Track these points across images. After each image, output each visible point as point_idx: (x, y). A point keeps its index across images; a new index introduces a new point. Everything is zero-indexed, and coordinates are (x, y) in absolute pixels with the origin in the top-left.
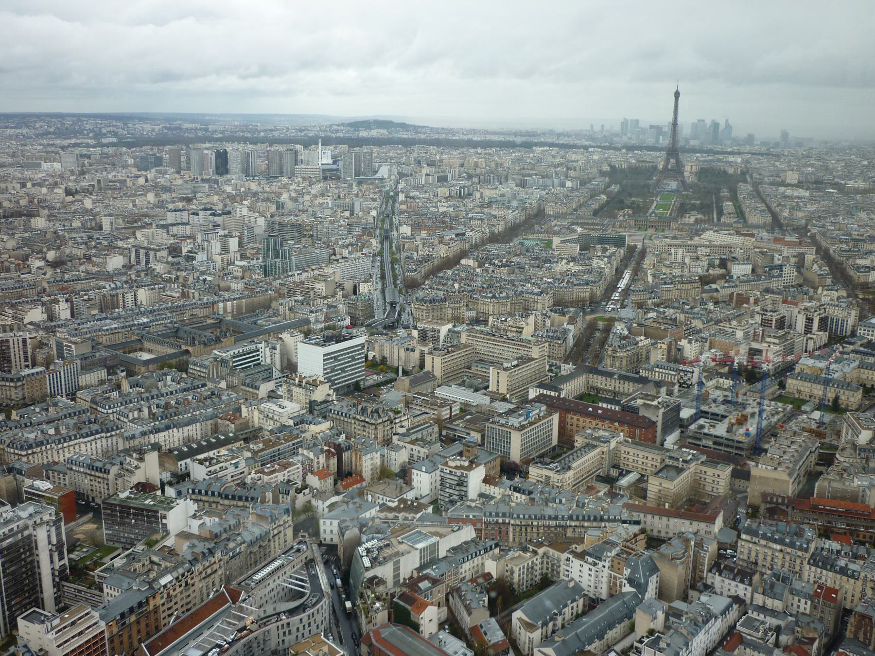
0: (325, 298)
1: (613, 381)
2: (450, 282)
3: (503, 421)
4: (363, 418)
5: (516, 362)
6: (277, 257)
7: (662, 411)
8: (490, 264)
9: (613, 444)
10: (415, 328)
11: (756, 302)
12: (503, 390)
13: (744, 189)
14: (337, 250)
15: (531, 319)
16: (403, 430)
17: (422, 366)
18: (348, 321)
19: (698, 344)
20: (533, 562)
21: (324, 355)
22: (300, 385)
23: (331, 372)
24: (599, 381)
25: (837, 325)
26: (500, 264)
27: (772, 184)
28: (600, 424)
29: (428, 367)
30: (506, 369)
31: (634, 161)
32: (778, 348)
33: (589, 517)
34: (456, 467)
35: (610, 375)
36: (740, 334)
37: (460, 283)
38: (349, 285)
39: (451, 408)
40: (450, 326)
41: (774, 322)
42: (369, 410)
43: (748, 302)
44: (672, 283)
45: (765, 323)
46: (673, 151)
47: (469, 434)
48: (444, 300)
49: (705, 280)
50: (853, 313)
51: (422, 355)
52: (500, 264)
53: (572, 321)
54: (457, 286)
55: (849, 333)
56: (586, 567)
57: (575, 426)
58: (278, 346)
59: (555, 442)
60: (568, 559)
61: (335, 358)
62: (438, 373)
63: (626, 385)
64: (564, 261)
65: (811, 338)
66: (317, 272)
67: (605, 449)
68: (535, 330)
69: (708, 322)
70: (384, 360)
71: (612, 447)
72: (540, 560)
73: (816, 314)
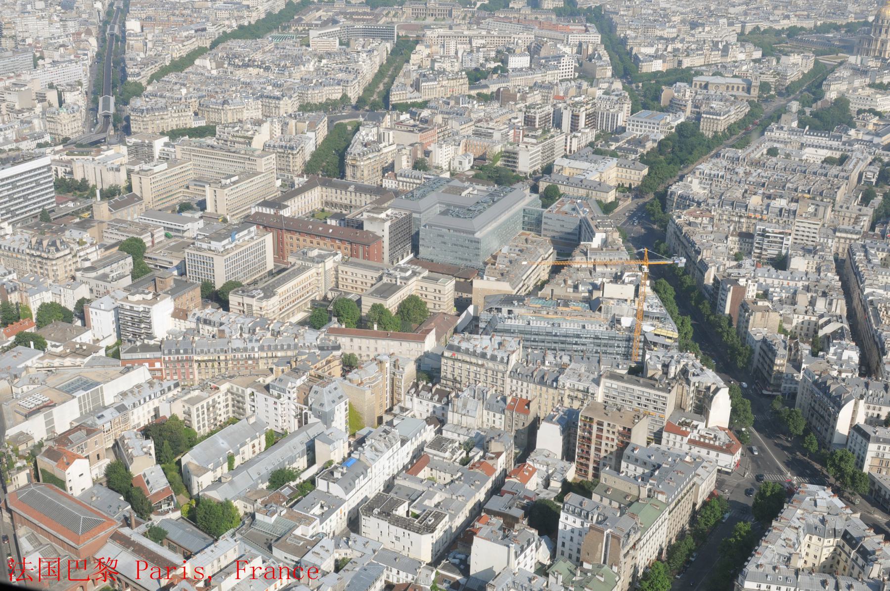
0: (21, 111)
1: (348, 193)
2: (178, 86)
4: (38, 253)
5: (236, 178)
7: (388, 224)
10: (125, 144)
12: (222, 211)
14: (46, 53)
16: (87, 264)
17: (129, 188)
20: (214, 400)
23: (10, 201)
28: (322, 242)
29: (136, 190)
33: (282, 346)
34: (138, 302)
35: (345, 187)
37: (188, 88)
38: (52, 96)
39: (152, 236)
41: (537, 120)
43: (514, 99)
51: (129, 172)
56: (271, 400)
57: (295, 245)
60: (253, 394)
61: (14, 185)
62: (148, 196)
66: (13, 81)
68: (271, 138)
70: (84, 181)
72: (223, 398)
73: (583, 109)
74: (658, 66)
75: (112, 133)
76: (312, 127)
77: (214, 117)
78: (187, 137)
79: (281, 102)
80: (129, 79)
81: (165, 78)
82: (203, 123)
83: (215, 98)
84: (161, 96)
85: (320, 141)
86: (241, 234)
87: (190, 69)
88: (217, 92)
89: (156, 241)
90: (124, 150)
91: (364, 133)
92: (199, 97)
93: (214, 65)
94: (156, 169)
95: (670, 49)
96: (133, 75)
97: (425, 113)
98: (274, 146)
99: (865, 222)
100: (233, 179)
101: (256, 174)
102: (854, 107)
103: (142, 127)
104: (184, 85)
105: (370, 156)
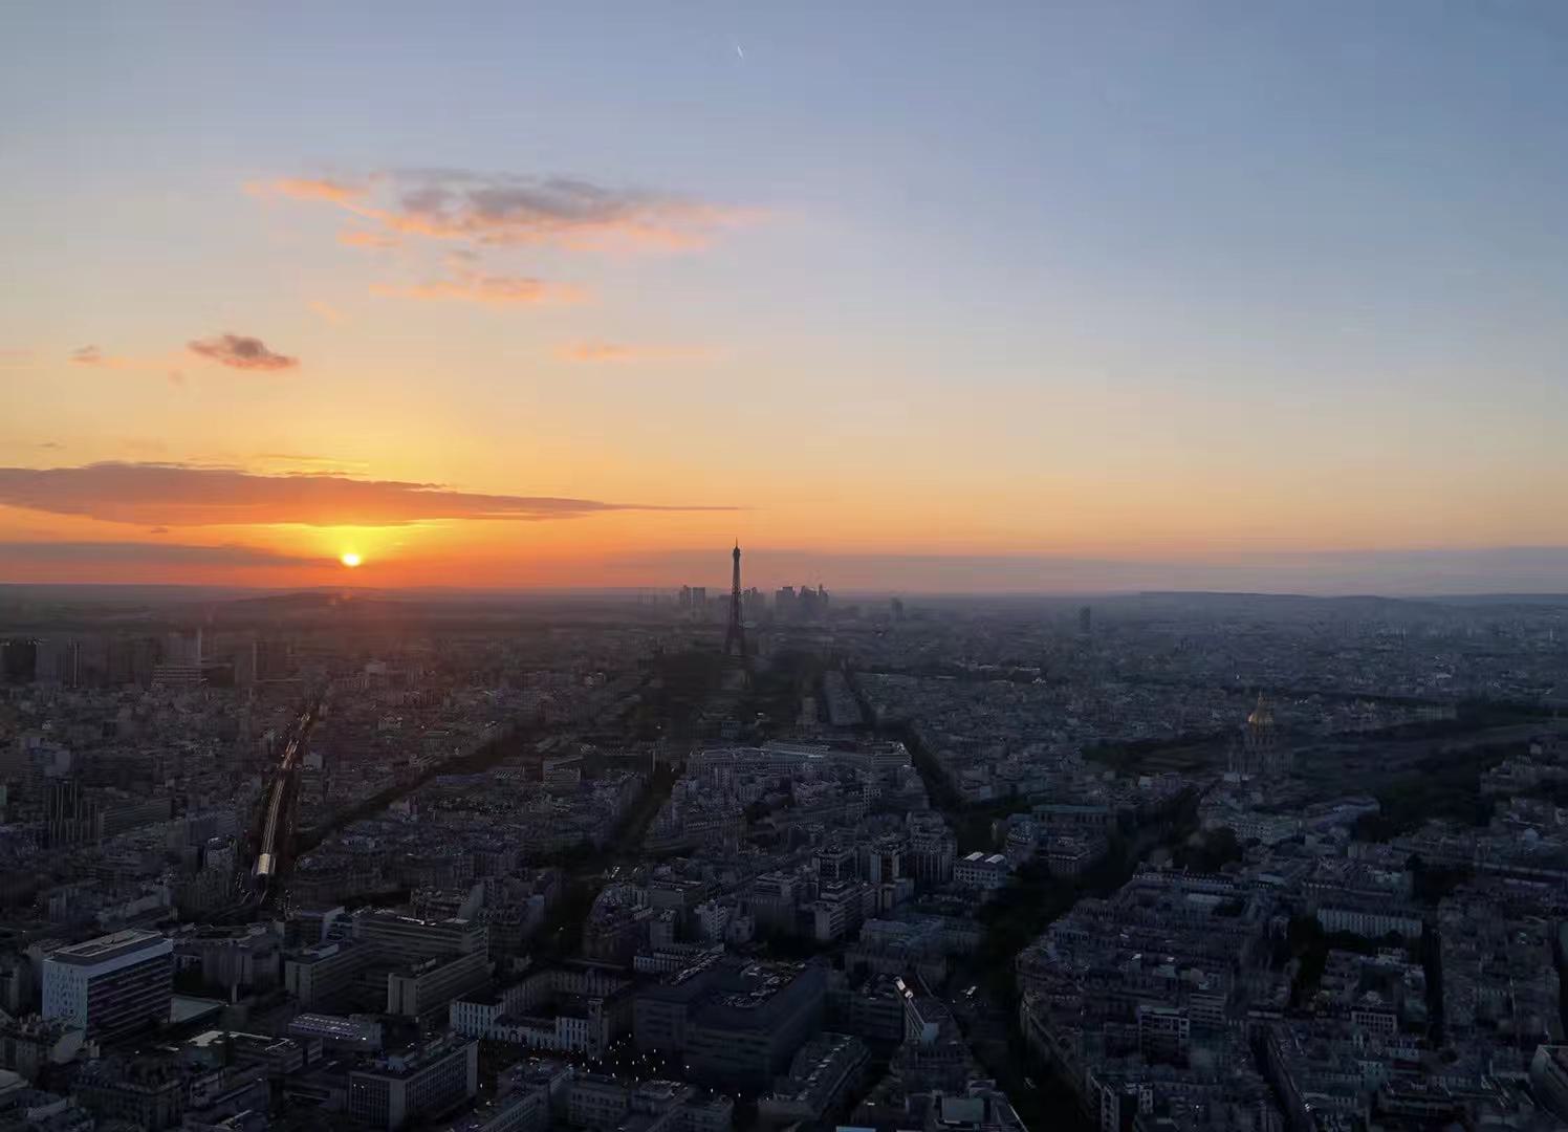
3: (379, 1064)
6: (69, 813)
8: (436, 807)
9: (555, 1084)
11: (819, 841)
12: (410, 1009)
13: (833, 681)
14: (190, 797)
15: (479, 889)
16: (204, 1100)
18: (174, 914)
19: (724, 910)
21: (90, 981)
22: (29, 1039)
24: (567, 981)
25: (928, 867)
26: (450, 806)
27: (875, 670)
30: (413, 976)
31: (688, 646)
32: (836, 908)
35: (582, 970)
36: (786, 889)
40: (340, 910)
42: (144, 1072)
44: (704, 820)
45: (826, 871)
46: (735, 631)
47: (327, 1094)
49: (756, 812)
50: (950, 846)
52: (450, 806)
53: (540, 889)
54: (372, 845)
55: (944, 878)
58: (16, 971)
59: (473, 1084)
61: (113, 985)
63: (607, 984)
64: (550, 796)
65: (889, 889)
67: (541, 1096)
68: (485, 905)
69: (745, 874)
71: (552, 1090)
73: (894, 852)
74: (986, 793)
86: (433, 1044)
87: (383, 815)
89: (310, 1060)
91: (609, 893)
93: (415, 808)
94: (322, 953)
95: (998, 771)
97: (691, 864)
99: (1284, 991)
100: (428, 964)
101: (459, 955)
102: (1242, 836)
105: (617, 925)
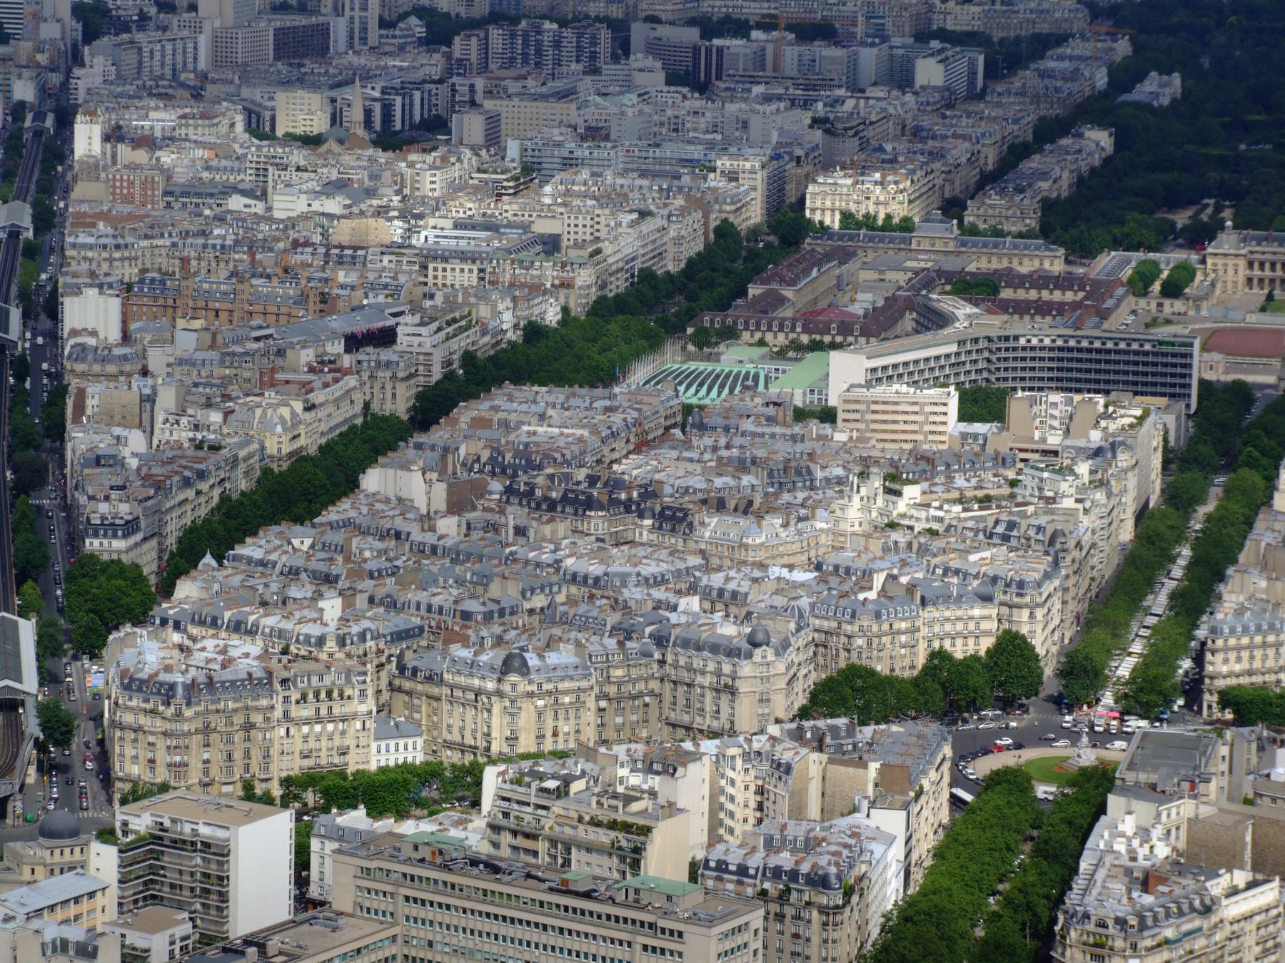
10: (107, 835)
37: (348, 596)
48: (262, 683)
75: (32, 775)
76: (898, 787)
77: (458, 722)
78: (361, 811)
79: (746, 669)
80: (93, 544)
81: (251, 549)
82: (411, 751)
83: (465, 641)
84: (238, 627)
85: (926, 843)
88: (467, 616)
90: (104, 861)
91: (1128, 825)
92: (398, 636)
93: (440, 490)
96: (110, 528)
98: (742, 870)
103: (162, 757)
104: (329, 580)
